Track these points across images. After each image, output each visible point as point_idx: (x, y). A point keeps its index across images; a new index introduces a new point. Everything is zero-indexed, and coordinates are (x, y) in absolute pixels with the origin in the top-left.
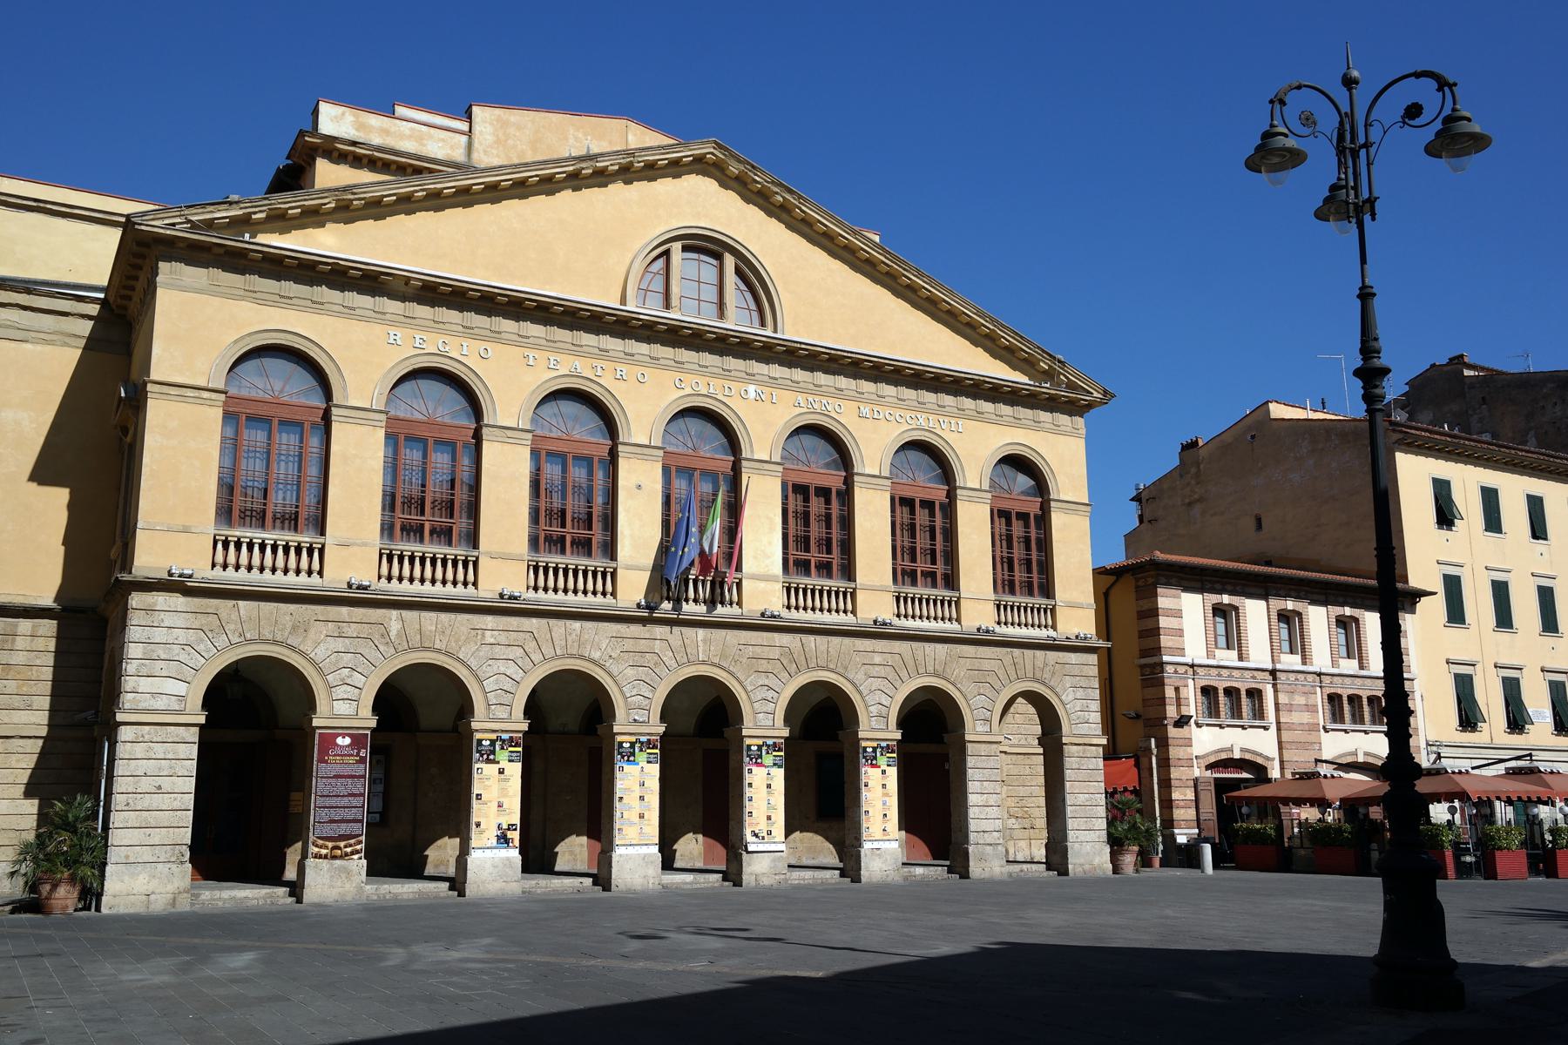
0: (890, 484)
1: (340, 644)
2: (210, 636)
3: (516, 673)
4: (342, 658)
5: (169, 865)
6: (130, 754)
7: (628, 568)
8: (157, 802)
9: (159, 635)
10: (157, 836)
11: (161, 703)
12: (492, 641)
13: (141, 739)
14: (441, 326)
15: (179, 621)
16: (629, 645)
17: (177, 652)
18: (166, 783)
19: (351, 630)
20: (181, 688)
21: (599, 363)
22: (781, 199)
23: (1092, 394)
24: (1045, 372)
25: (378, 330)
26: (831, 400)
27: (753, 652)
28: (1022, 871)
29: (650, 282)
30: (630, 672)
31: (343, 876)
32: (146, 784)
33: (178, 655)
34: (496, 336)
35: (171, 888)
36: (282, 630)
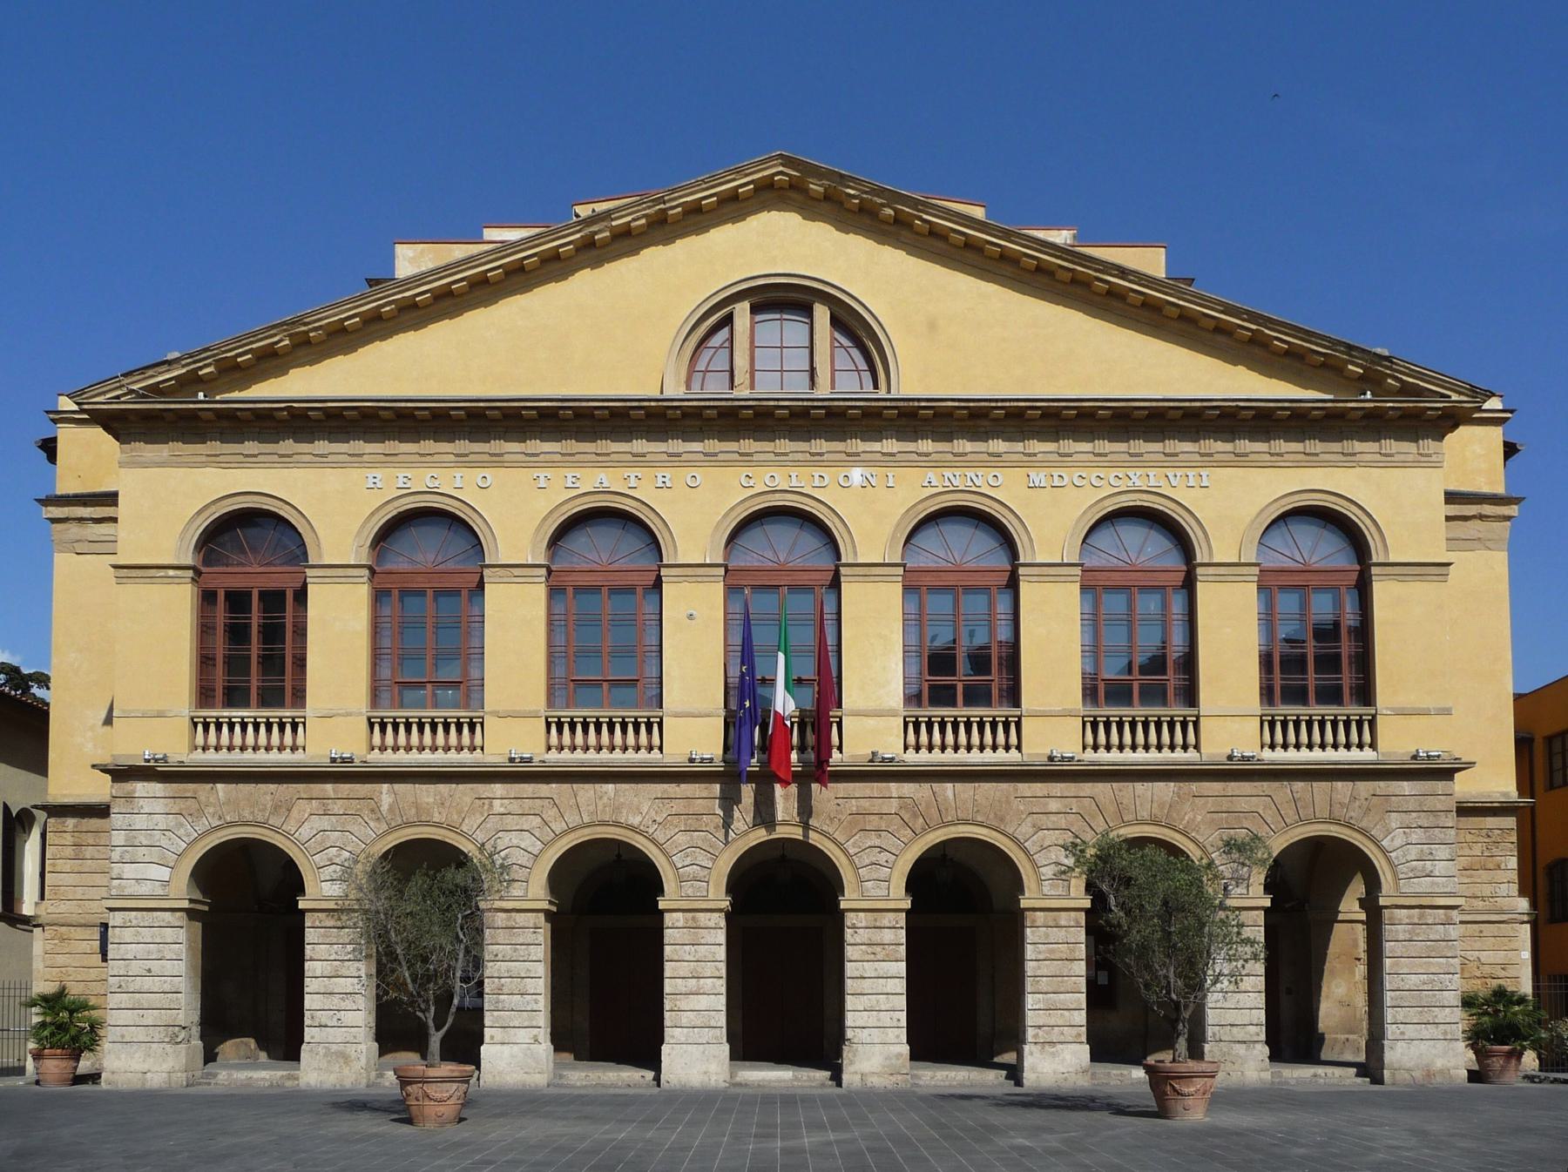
0: (1080, 573)
1: (325, 823)
2: (190, 820)
3: (533, 845)
4: (328, 835)
5: (162, 1045)
6: (120, 938)
7: (677, 715)
8: (148, 983)
9: (140, 822)
10: (150, 1017)
11: (145, 889)
12: (502, 810)
13: (129, 924)
14: (428, 458)
15: (159, 806)
16: (677, 807)
17: (157, 837)
18: (156, 966)
19: (337, 807)
20: (164, 873)
21: (632, 472)
22: (892, 213)
23: (1450, 397)
24: (1361, 378)
25: (355, 474)
26: (980, 472)
27: (857, 807)
28: (1315, 1076)
29: (710, 360)
30: (682, 839)
31: (342, 1061)
32: (136, 968)
33: (159, 840)
34: (497, 461)
35: (166, 1066)
36: (264, 810)
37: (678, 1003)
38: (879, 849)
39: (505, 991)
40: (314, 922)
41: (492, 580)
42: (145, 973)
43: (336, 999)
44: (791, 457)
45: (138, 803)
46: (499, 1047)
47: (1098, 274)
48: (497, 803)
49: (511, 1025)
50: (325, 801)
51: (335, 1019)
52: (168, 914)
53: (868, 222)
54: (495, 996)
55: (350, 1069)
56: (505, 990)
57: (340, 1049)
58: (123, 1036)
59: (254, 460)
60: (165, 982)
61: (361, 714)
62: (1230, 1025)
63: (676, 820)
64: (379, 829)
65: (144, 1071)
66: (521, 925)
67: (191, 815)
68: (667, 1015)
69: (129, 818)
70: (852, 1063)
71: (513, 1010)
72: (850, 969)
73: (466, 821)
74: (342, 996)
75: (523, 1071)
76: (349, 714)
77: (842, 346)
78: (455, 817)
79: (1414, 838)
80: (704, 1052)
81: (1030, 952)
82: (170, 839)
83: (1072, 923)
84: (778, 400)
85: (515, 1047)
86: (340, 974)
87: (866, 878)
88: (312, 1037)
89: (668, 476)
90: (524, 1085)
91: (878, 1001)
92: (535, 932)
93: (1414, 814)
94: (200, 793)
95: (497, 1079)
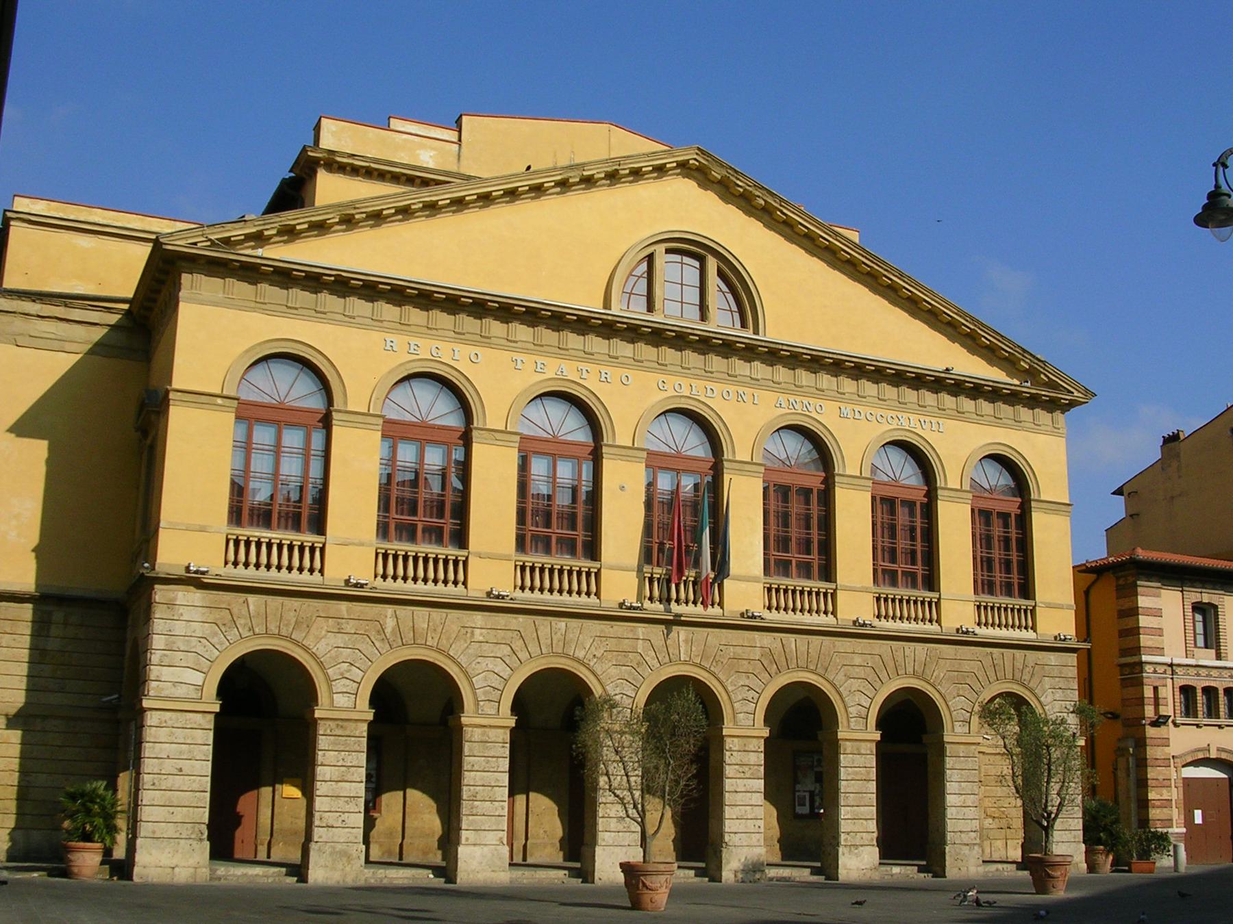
0: (871, 485)
1: (340, 640)
2: (223, 630)
3: (504, 671)
4: (341, 653)
5: (190, 842)
6: (155, 737)
7: (611, 568)
8: (178, 781)
9: (179, 628)
10: (180, 815)
11: (180, 691)
12: (481, 639)
13: (164, 725)
14: (434, 332)
15: (196, 614)
16: (612, 644)
17: (194, 644)
18: (186, 766)
19: (350, 627)
20: (197, 678)
21: (582, 366)
22: (763, 203)
23: (1073, 393)
24: (1026, 371)
25: (376, 336)
26: (812, 401)
27: (734, 653)
28: (997, 870)
29: (634, 286)
30: (614, 671)
31: (345, 859)
32: (169, 766)
33: (195, 647)
34: (485, 340)
35: (192, 862)
36: (287, 625)
37: (608, 811)
38: (747, 688)
39: (478, 798)
40: (325, 730)
41: (479, 440)
42: (176, 772)
43: (341, 801)
44: (692, 371)
45: (179, 610)
46: (472, 848)
47: (886, 273)
48: (477, 632)
49: (483, 828)
50: (339, 620)
51: (340, 821)
52: (199, 716)
53: (744, 205)
54: (471, 802)
55: (352, 867)
56: (479, 797)
57: (344, 848)
58: (154, 832)
59: (295, 312)
60: (194, 781)
61: (371, 545)
62: (960, 832)
63: (609, 655)
64: (383, 648)
65: (173, 866)
66: (493, 740)
67: (224, 625)
68: (600, 821)
69: (169, 623)
70: (728, 862)
71: (484, 815)
72: (728, 784)
73: (453, 646)
74: (346, 799)
75: (490, 870)
76: (362, 544)
77: (721, 291)
78: (445, 642)
79: (1057, 696)
80: (626, 853)
81: (843, 774)
82: (205, 647)
83: (868, 752)
84: (693, 329)
85: (486, 849)
86: (346, 779)
87: (739, 711)
88: (320, 837)
89: (609, 373)
90: (492, 883)
91: (746, 811)
92: (503, 747)
93: (1057, 679)
94: (234, 605)
95: (471, 876)
